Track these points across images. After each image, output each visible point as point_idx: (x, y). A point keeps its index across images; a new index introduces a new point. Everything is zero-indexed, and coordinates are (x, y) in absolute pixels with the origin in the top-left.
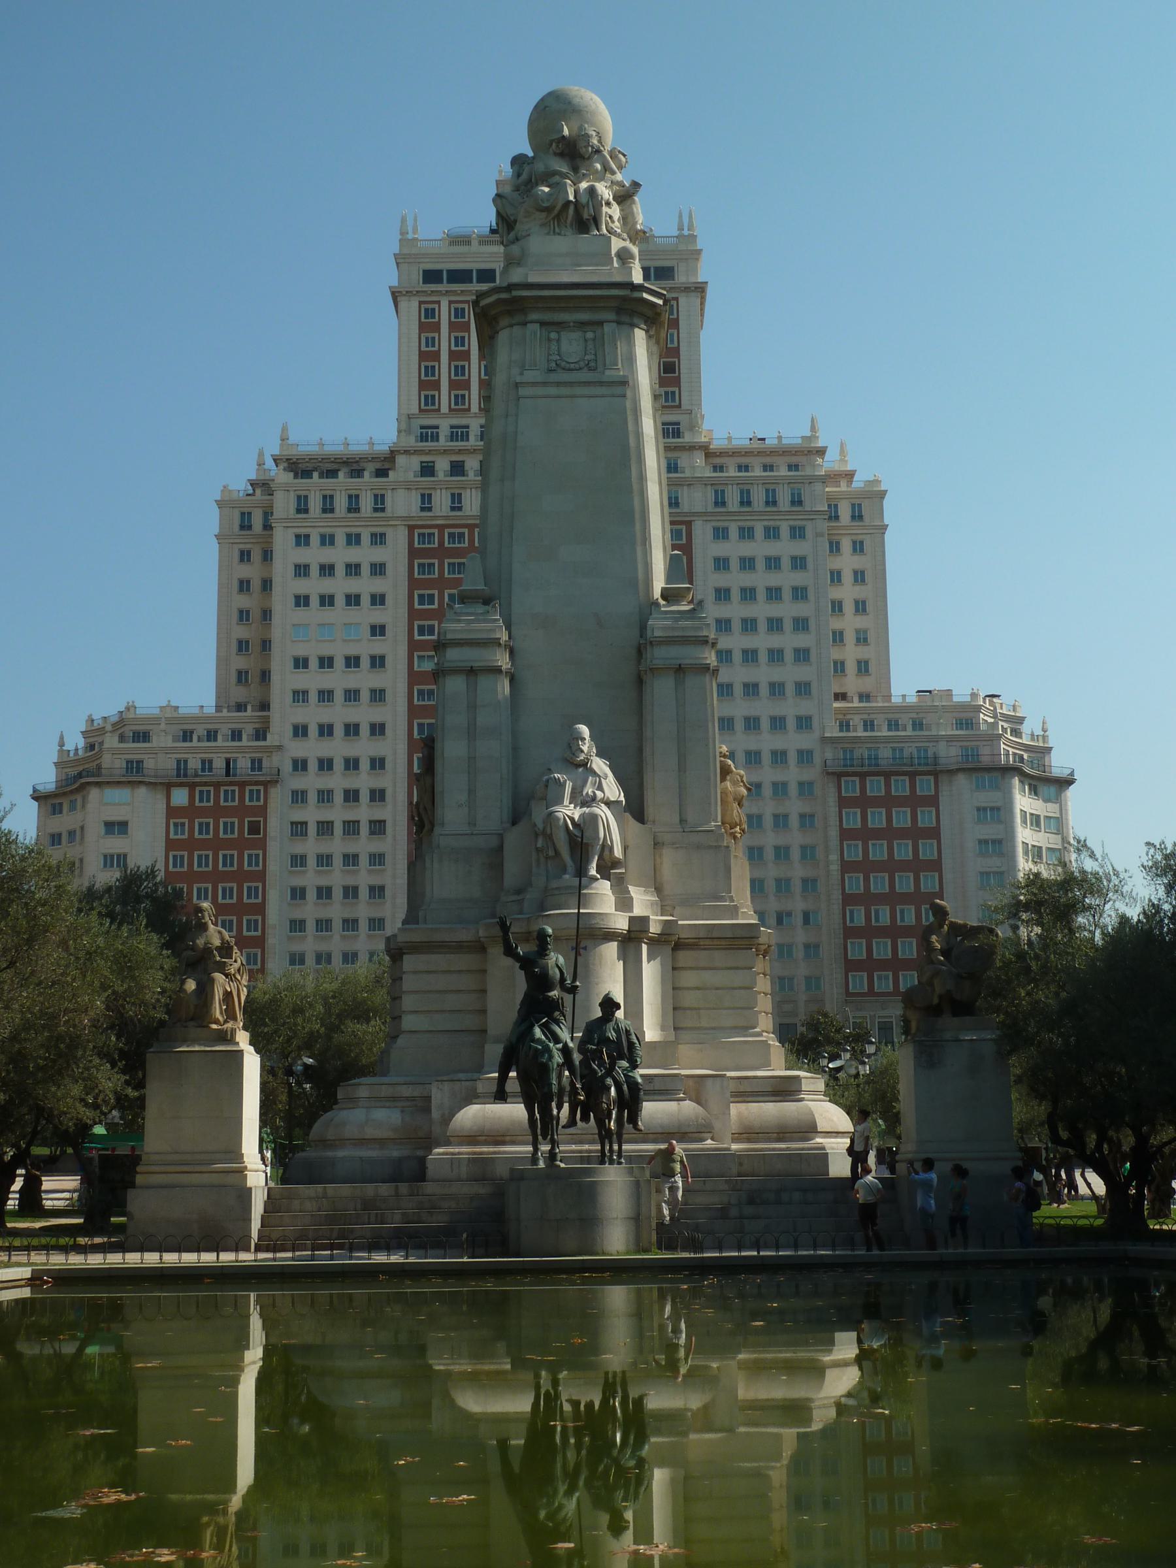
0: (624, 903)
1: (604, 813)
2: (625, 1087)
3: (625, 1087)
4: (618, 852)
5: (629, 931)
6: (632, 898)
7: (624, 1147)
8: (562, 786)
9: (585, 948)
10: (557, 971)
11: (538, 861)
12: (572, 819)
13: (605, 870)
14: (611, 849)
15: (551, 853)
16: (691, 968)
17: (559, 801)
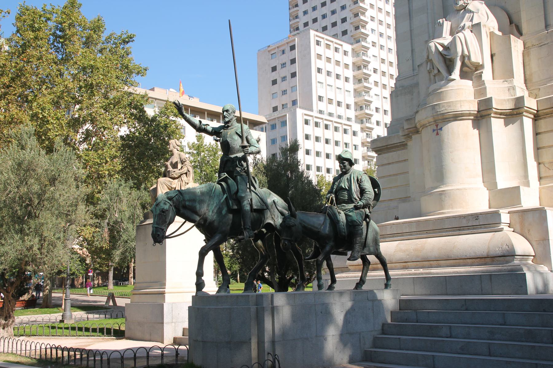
4: (475, 58)
5: (478, 111)
7: (391, 273)
12: (442, 45)
14: (469, 57)
15: (436, 71)
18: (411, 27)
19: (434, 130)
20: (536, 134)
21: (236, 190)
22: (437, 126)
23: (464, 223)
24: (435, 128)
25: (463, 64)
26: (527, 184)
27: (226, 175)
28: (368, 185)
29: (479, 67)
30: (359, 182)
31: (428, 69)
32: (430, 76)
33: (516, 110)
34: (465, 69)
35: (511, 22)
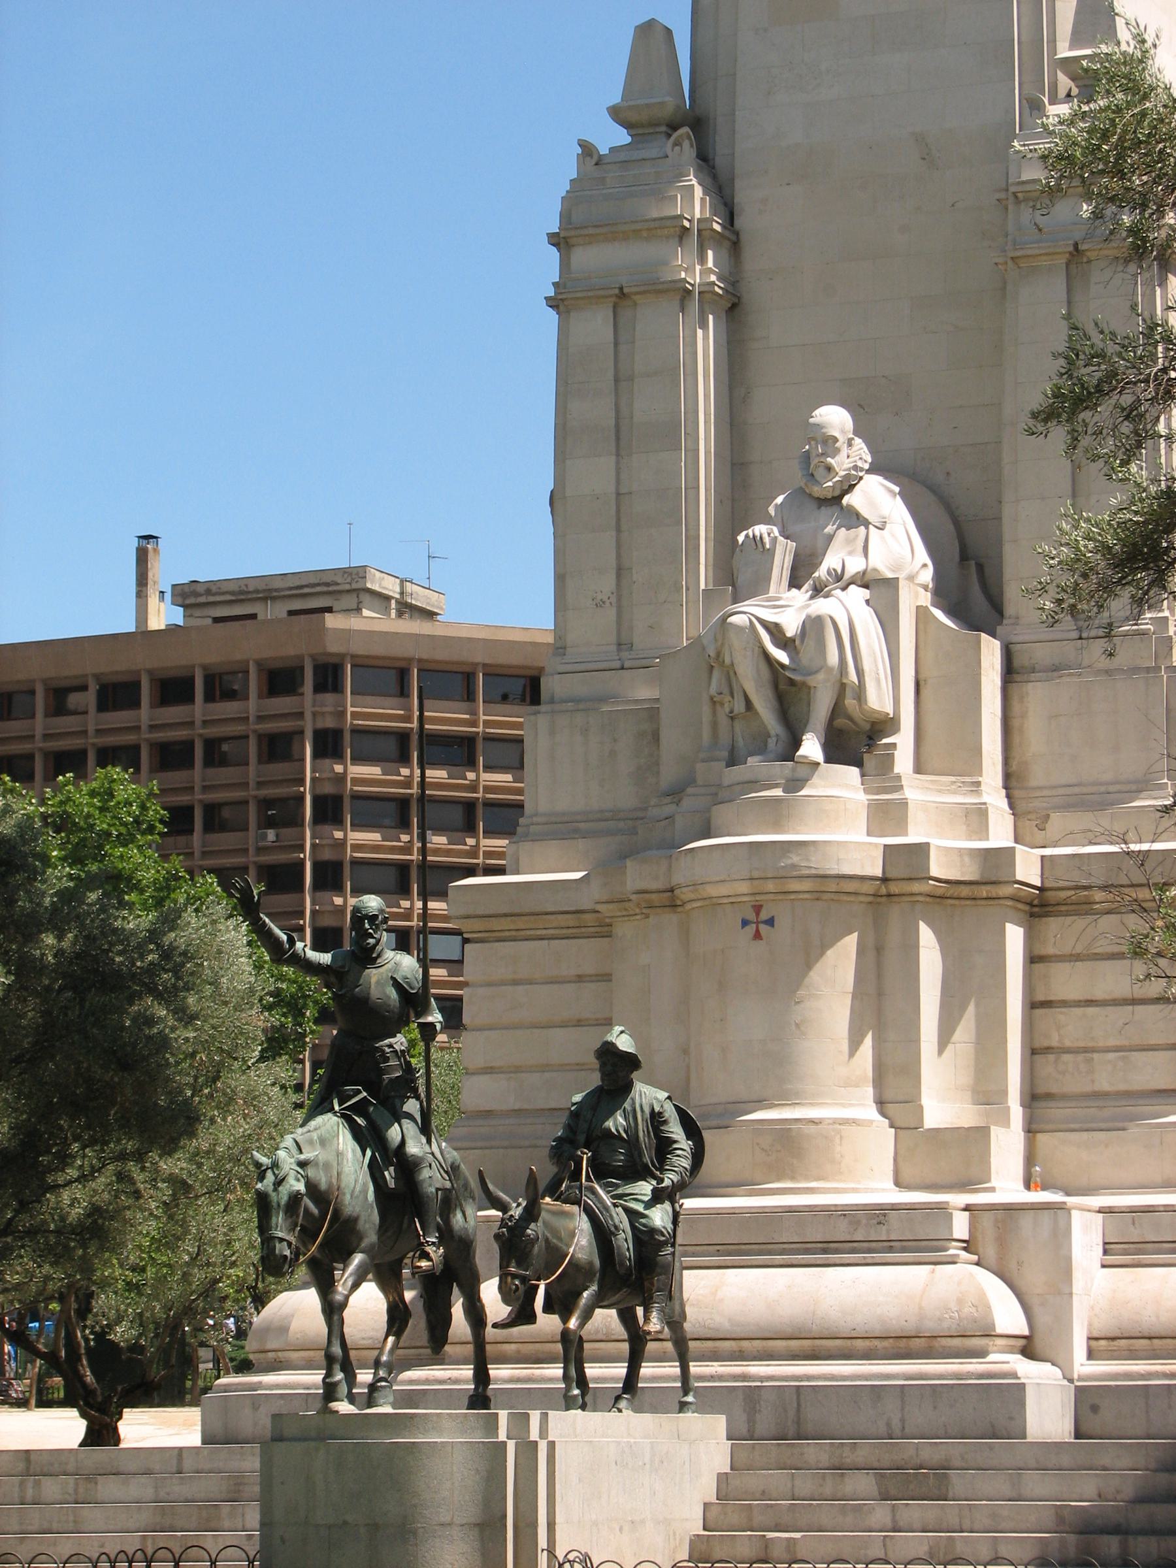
0: (888, 813)
1: (850, 607)
2: (624, 1242)
3: (624, 1242)
4: (878, 699)
6: (904, 804)
8: (771, 553)
9: (770, 922)
10: (393, 994)
11: (714, 725)
12: (775, 631)
13: (856, 740)
14: (860, 693)
15: (739, 707)
16: (1076, 958)
17: (758, 586)
18: (618, 482)
19: (745, 923)
20: (1033, 959)
21: (399, 1138)
22: (758, 909)
23: (841, 1231)
24: (751, 916)
25: (837, 709)
26: (1006, 1123)
27: (365, 1094)
28: (676, 1131)
29: (883, 726)
30: (657, 1119)
31: (713, 690)
32: (714, 713)
33: (988, 887)
34: (840, 722)
35: (964, 557)
